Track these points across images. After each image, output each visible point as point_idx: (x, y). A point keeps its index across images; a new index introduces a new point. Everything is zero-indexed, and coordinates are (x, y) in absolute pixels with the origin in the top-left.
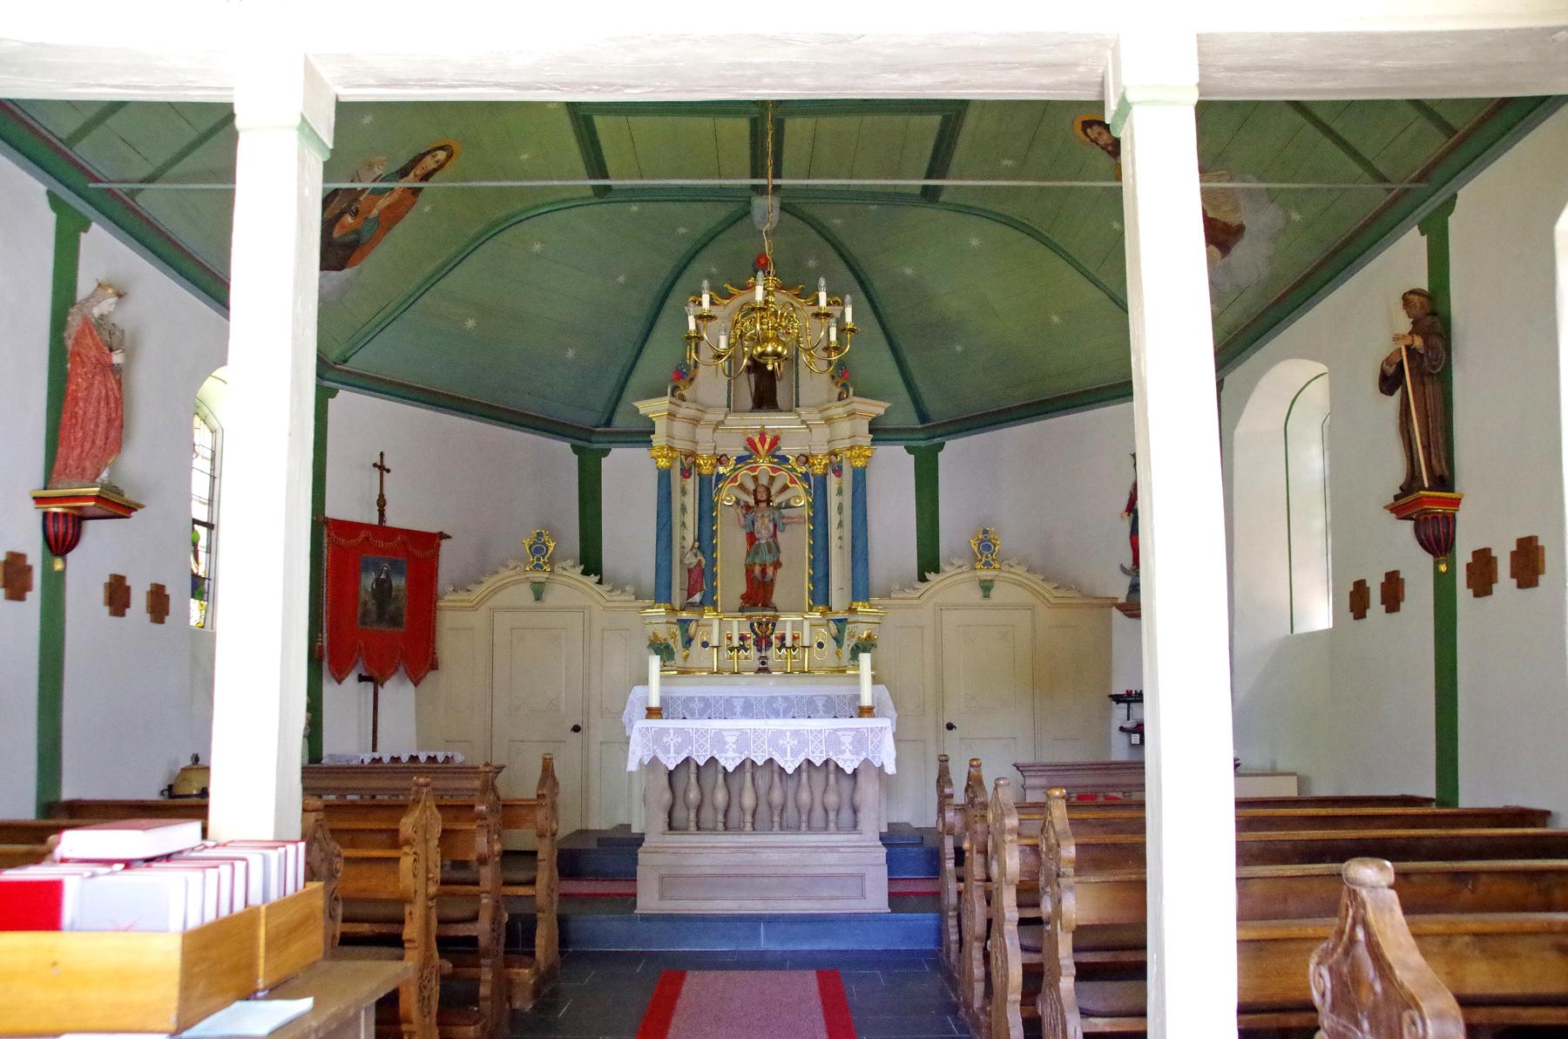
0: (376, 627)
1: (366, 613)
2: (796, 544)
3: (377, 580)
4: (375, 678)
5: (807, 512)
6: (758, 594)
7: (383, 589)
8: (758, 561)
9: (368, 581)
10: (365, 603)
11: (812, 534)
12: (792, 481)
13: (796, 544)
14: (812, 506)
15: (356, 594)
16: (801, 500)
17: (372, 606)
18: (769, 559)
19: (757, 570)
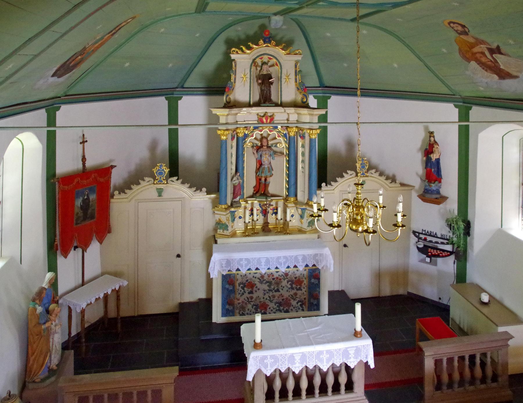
0: (84, 223)
1: (77, 219)
2: (279, 166)
3: (84, 201)
4: (84, 245)
5: (285, 151)
6: (261, 190)
7: (86, 204)
8: (263, 175)
9: (78, 202)
10: (78, 213)
11: (288, 162)
12: (279, 136)
13: (279, 166)
14: (289, 149)
15: (73, 211)
16: (282, 146)
17: (81, 214)
18: (268, 174)
19: (263, 179)
